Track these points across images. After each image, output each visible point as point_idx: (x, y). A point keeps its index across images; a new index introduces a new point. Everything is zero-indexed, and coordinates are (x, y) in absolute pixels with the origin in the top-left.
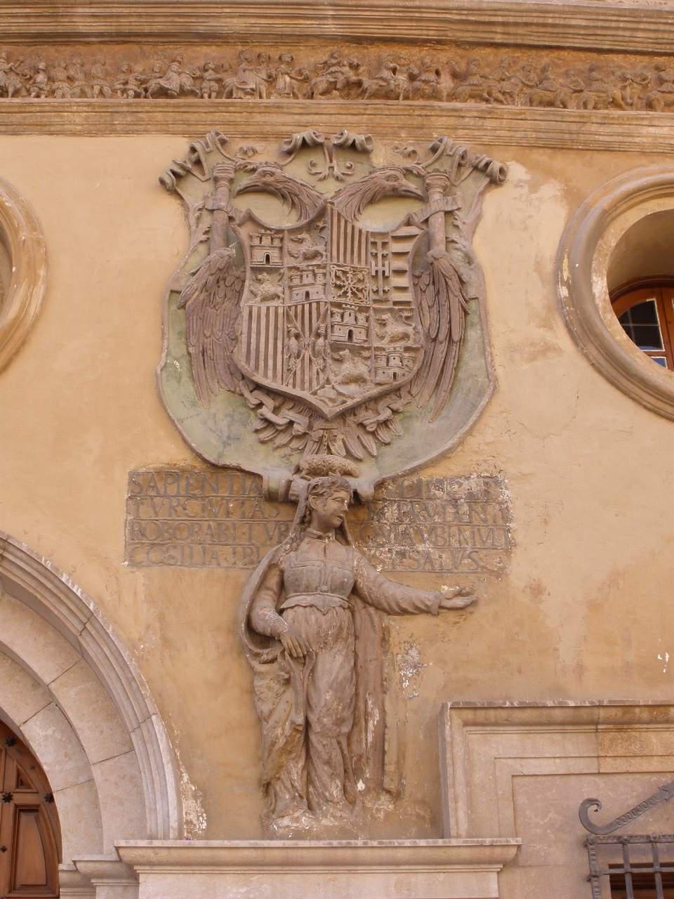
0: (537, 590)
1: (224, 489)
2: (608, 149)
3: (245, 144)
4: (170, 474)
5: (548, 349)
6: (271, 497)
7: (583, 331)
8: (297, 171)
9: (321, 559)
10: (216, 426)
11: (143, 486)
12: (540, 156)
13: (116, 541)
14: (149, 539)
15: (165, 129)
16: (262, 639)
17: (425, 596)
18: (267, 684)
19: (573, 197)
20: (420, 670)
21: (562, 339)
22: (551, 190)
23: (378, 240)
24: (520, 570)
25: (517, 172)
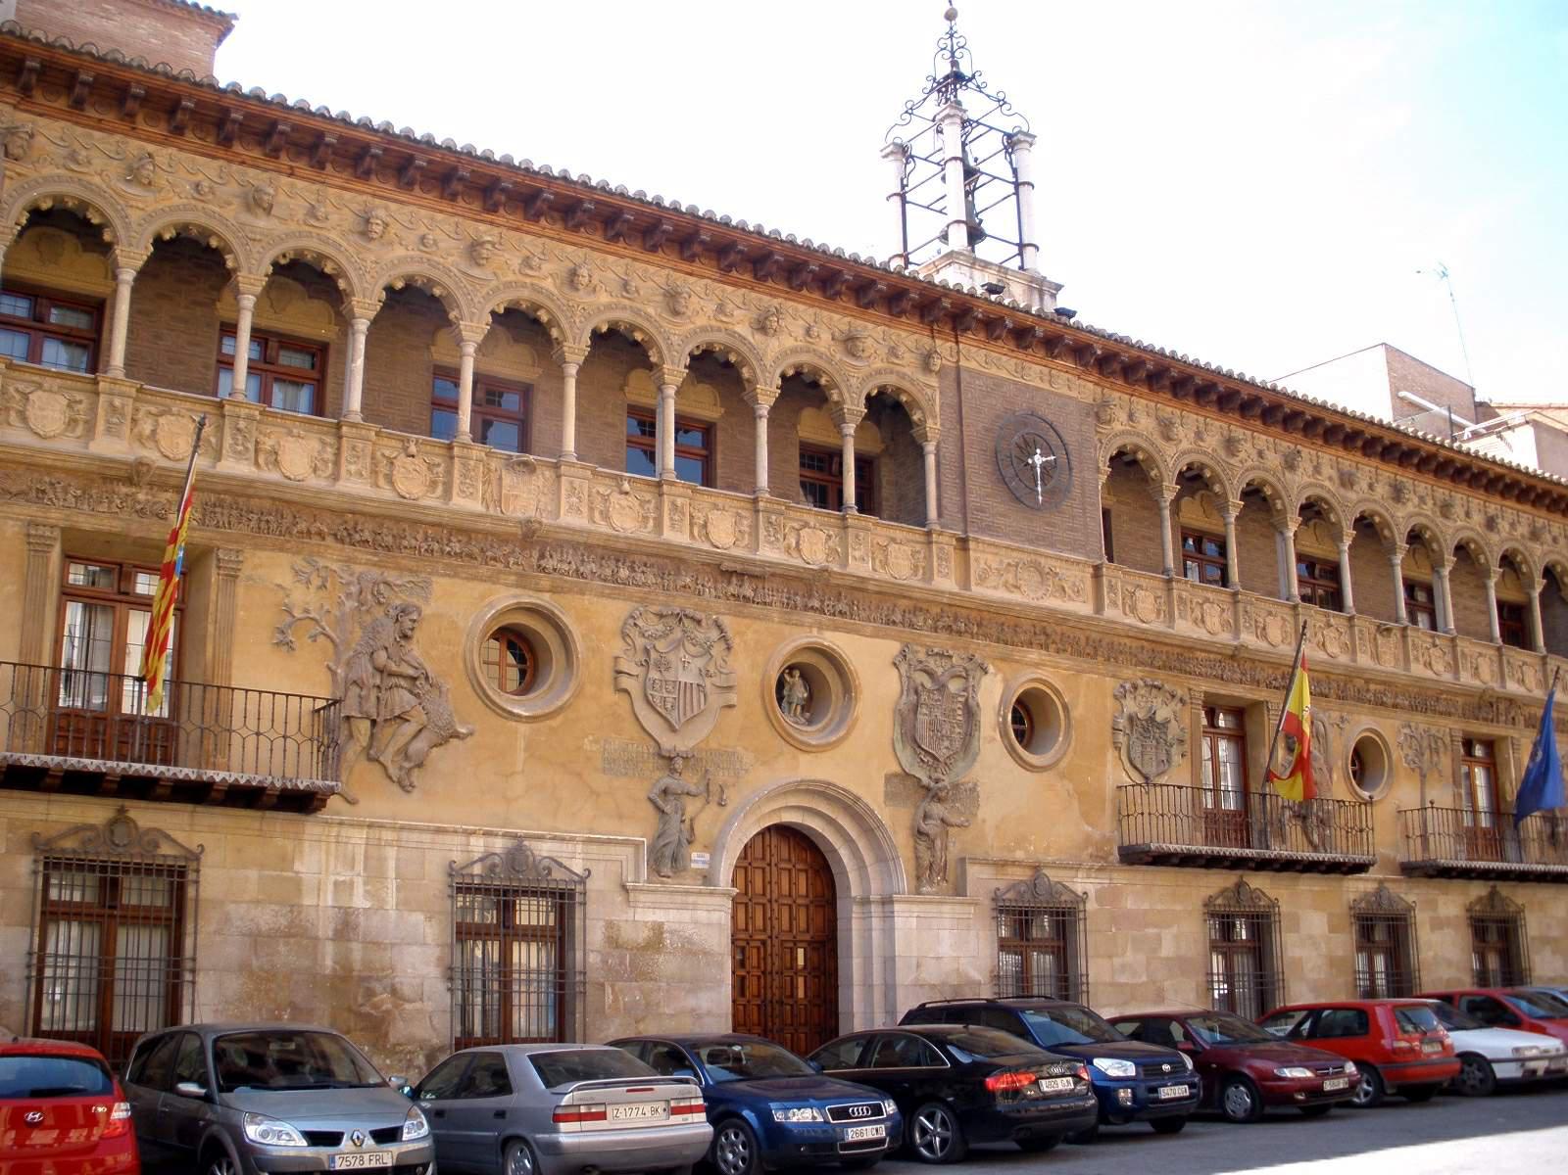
0: (984, 821)
1: (909, 782)
2: (1017, 661)
3: (916, 648)
4: (896, 775)
5: (994, 739)
6: (923, 787)
7: (1004, 735)
8: (932, 664)
9: (937, 809)
10: (907, 757)
11: (889, 778)
12: (998, 663)
13: (881, 798)
14: (890, 797)
15: (893, 638)
16: (920, 833)
17: (958, 822)
18: (922, 846)
19: (1006, 681)
20: (956, 846)
21: (998, 737)
22: (1000, 677)
23: (954, 696)
24: (981, 814)
25: (991, 669)
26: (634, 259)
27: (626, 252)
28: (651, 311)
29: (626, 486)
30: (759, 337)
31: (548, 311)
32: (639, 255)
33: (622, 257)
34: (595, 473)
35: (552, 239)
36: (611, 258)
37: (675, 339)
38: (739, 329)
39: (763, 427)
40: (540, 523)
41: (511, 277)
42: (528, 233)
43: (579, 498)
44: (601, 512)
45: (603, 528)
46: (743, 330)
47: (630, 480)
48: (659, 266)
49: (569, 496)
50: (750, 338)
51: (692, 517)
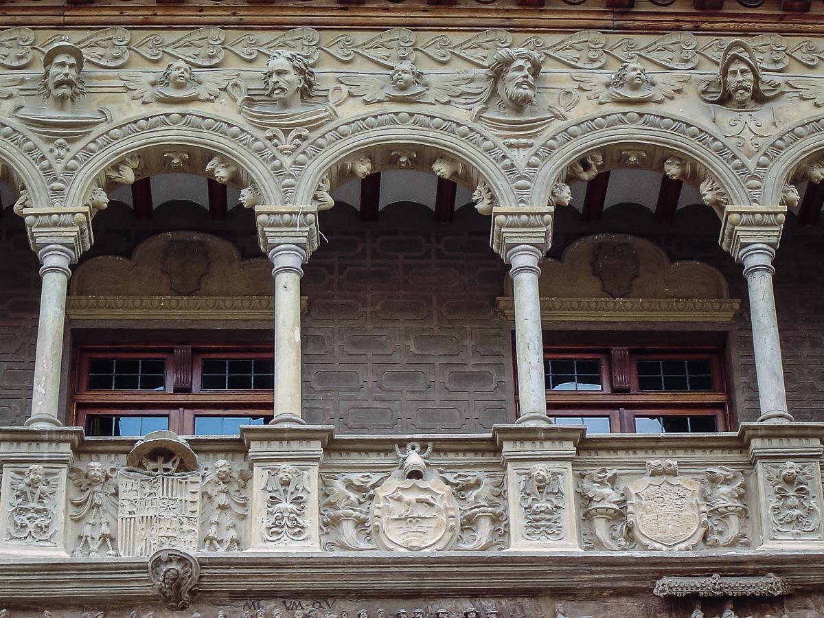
26: (415, 27)
27: (390, 17)
28: (459, 113)
29: (414, 459)
30: (726, 116)
31: (226, 160)
32: (420, 17)
33: (381, 27)
34: (332, 446)
35: (224, 26)
36: (360, 37)
37: (520, 158)
38: (673, 109)
39: (761, 290)
40: (183, 560)
41: (137, 111)
42: (170, 26)
43: (298, 500)
44: (361, 524)
45: (365, 549)
46: (688, 108)
47: (424, 443)
48: (471, 28)
49: (273, 500)
50: (706, 123)
51: (584, 499)
